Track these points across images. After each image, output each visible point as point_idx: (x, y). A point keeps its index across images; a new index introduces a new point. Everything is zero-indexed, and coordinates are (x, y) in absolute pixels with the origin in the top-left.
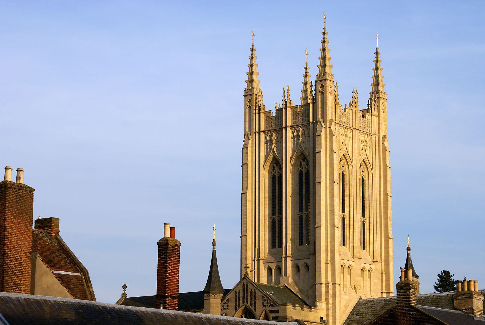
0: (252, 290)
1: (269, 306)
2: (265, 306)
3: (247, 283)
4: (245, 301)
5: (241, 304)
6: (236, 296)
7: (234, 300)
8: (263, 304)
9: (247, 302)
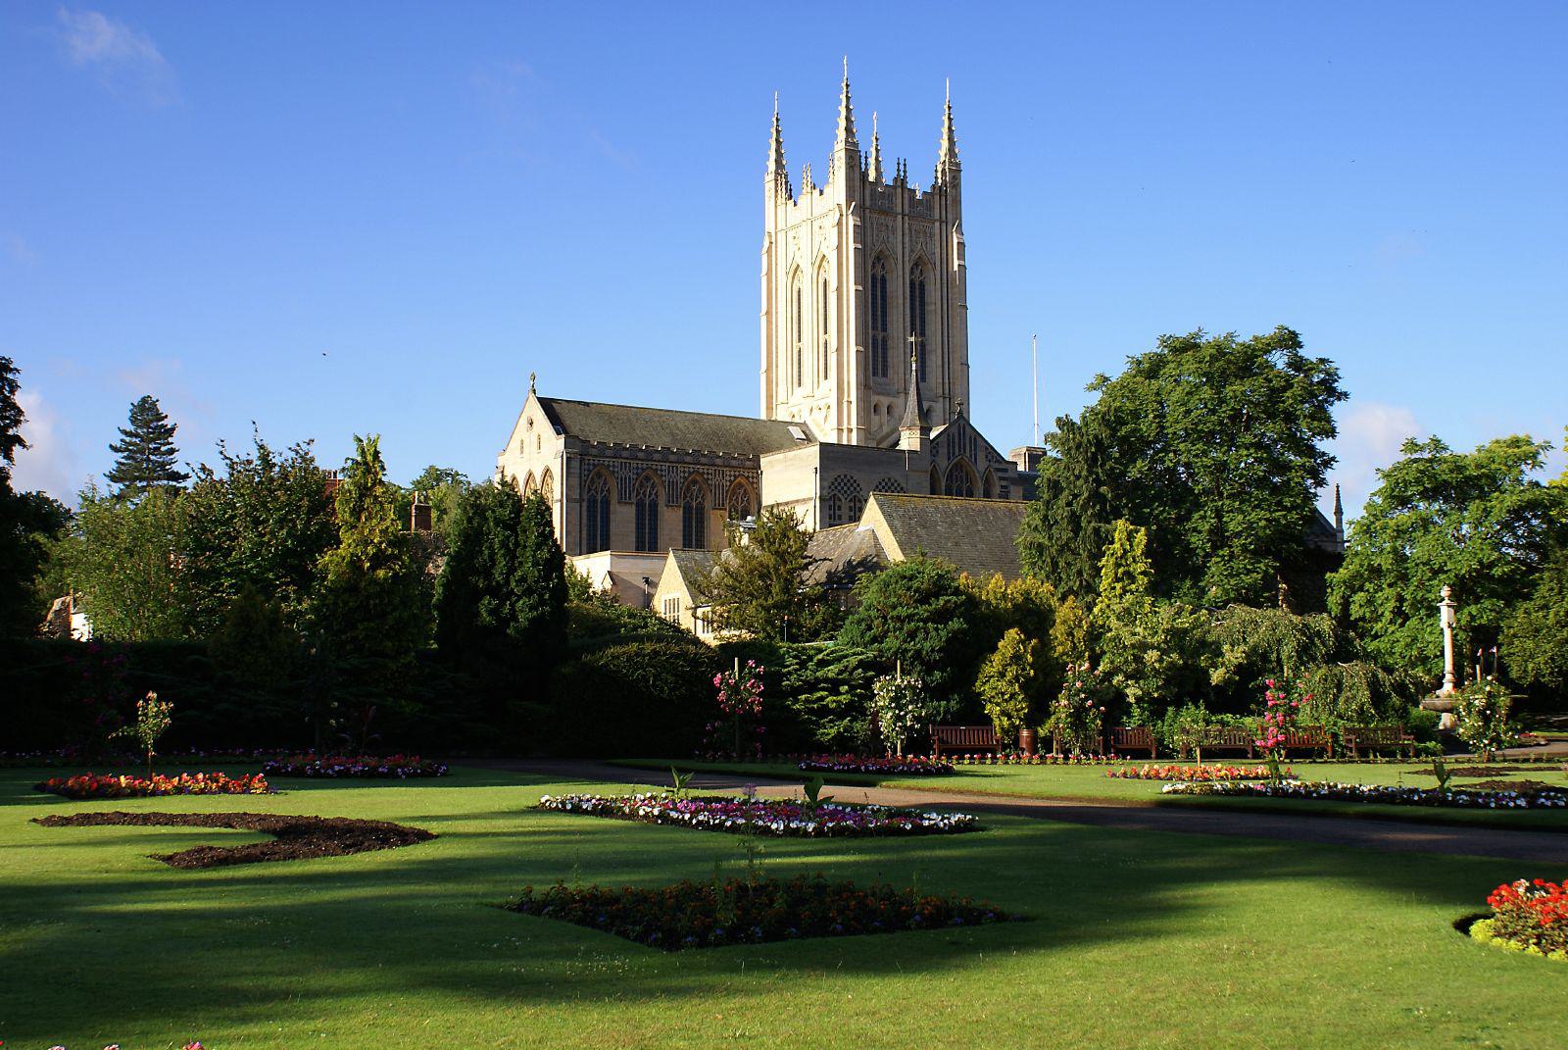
5: (957, 453)
6: (949, 440)
7: (946, 446)
8: (987, 457)
9: (965, 452)
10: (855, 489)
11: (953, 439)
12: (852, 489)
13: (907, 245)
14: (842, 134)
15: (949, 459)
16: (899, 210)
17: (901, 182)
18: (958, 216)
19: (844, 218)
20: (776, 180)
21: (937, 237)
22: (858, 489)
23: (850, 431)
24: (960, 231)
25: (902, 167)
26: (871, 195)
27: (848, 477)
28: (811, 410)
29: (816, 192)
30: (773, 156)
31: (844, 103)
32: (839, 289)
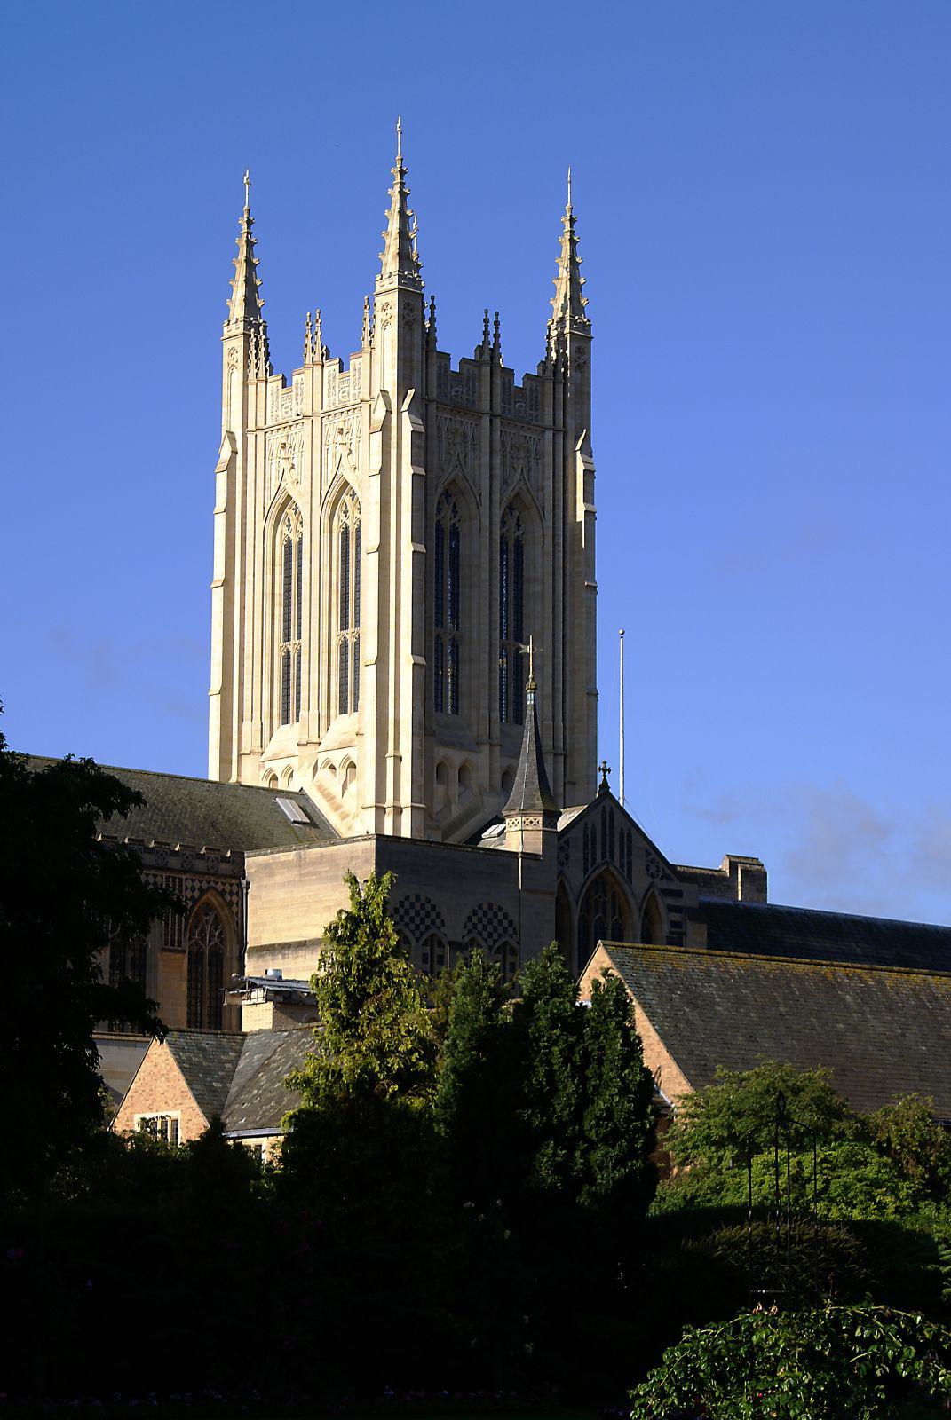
0: (622, 829)
1: (662, 878)
2: (653, 876)
3: (611, 808)
4: (608, 855)
5: (599, 860)
6: (586, 835)
7: (581, 844)
8: (648, 869)
9: (612, 856)
10: (433, 922)
11: (594, 834)
12: (428, 921)
13: (498, 472)
14: (391, 263)
15: (586, 870)
16: (486, 406)
17: (489, 353)
18: (584, 422)
19: (394, 417)
20: (247, 336)
21: (548, 459)
22: (438, 922)
23: (398, 811)
24: (587, 450)
25: (492, 325)
26: (439, 378)
27: (423, 900)
28: (315, 769)
29: (332, 367)
30: (239, 291)
31: (396, 206)
32: (383, 549)
